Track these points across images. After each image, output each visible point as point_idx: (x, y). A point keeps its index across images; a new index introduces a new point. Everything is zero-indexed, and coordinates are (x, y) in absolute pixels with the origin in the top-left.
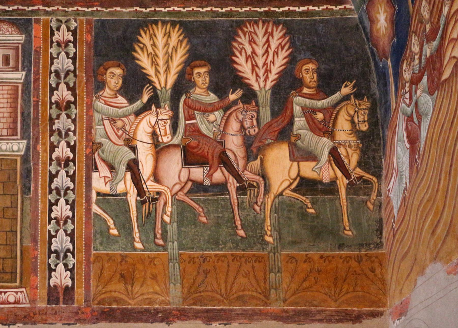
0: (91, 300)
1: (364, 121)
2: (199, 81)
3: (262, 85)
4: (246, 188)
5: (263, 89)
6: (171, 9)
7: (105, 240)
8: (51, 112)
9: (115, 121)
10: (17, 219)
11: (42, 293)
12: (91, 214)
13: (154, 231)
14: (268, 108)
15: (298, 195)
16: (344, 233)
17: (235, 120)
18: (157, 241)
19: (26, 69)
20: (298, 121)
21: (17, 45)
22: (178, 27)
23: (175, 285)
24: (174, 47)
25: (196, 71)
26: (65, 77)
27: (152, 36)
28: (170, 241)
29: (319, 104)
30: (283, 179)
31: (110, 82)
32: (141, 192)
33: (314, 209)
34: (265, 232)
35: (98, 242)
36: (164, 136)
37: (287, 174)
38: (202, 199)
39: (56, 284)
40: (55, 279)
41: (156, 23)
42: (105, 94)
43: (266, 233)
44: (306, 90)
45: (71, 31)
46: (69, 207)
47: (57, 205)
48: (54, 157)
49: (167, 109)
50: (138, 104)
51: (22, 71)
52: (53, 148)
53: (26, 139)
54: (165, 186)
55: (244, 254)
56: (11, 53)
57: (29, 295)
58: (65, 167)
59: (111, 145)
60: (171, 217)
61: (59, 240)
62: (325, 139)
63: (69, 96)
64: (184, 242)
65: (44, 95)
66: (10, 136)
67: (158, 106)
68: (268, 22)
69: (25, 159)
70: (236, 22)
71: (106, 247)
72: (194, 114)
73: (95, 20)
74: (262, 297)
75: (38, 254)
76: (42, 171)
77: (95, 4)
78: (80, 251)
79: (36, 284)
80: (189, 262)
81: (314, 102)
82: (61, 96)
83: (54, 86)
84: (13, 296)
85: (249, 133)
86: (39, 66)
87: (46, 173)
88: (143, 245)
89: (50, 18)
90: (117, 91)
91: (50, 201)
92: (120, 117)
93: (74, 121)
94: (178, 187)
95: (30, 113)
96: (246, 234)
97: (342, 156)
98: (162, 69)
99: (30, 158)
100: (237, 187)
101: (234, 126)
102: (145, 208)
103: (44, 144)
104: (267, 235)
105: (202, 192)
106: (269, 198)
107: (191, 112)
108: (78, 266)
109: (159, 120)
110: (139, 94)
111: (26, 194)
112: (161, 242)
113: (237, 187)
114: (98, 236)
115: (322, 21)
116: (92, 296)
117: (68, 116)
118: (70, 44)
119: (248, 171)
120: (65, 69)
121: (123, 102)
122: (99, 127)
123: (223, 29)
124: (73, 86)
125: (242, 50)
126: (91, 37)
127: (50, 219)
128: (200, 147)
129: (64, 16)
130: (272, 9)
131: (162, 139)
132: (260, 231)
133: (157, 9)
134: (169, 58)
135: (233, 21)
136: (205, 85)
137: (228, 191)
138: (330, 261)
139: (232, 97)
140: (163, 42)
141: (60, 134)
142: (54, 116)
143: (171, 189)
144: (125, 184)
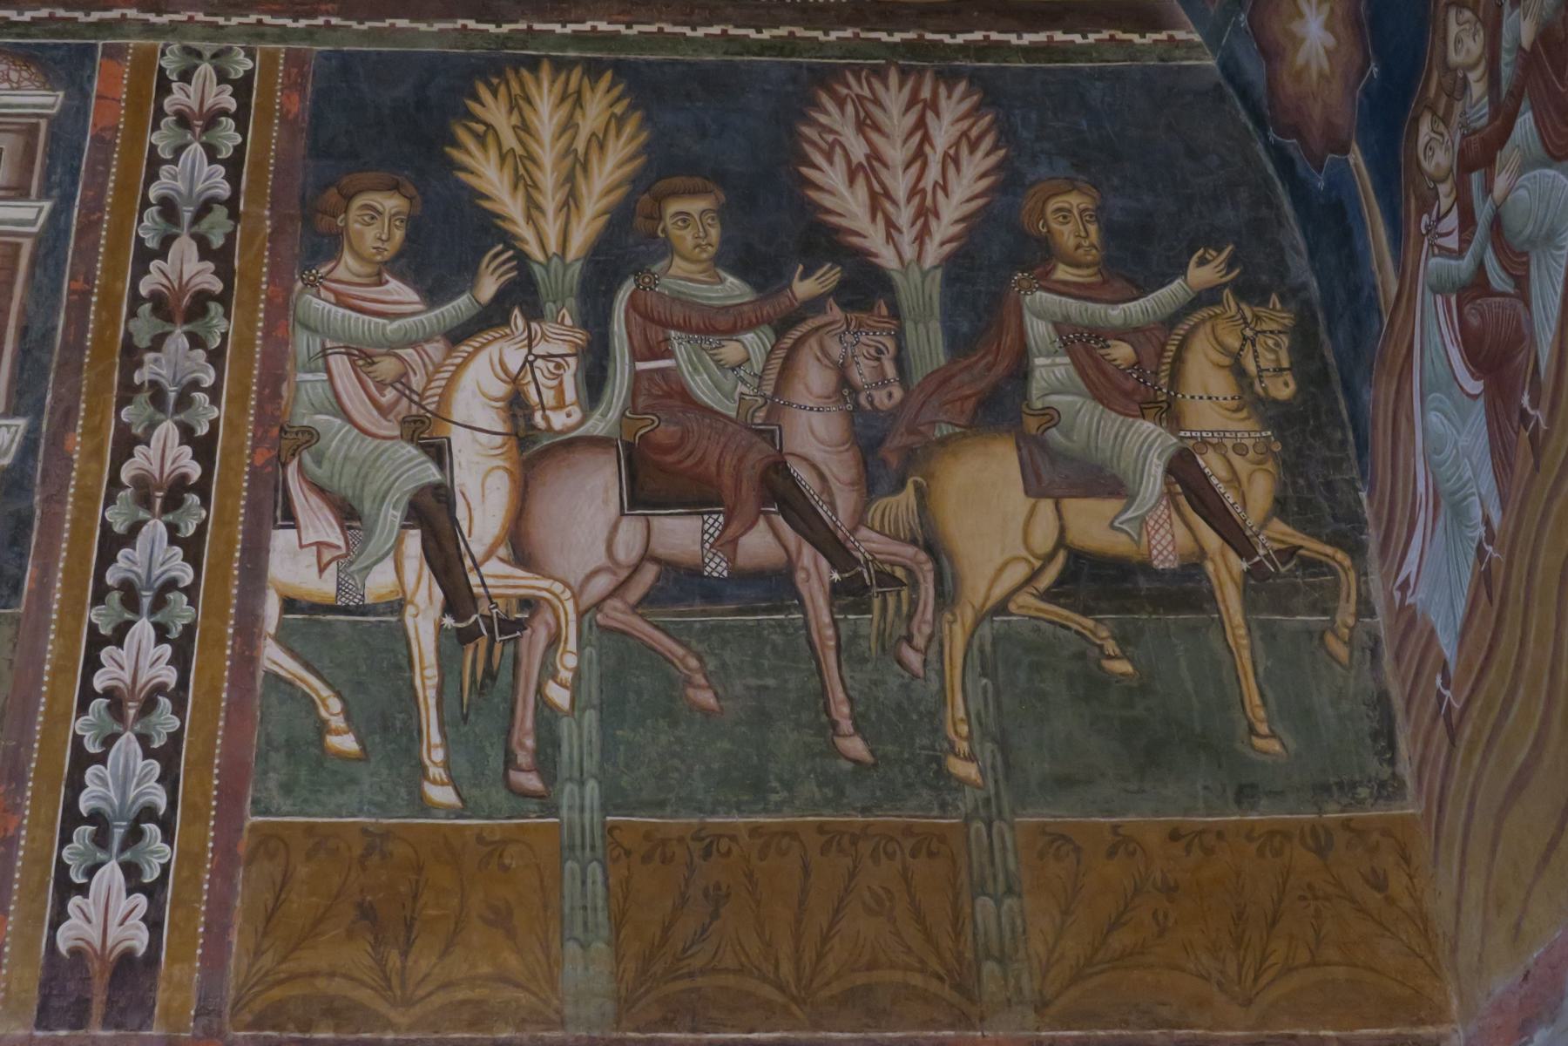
0: (227, 1010)
1: (1279, 370)
2: (686, 238)
3: (909, 252)
4: (866, 588)
5: (914, 268)
6: (587, 27)
7: (303, 774)
9: (369, 359)
12: (253, 676)
13: (508, 741)
14: (935, 325)
15: (1065, 612)
16: (1252, 746)
17: (819, 360)
18: (515, 776)
19: (55, 192)
20: (1043, 366)
21: (34, 120)
22: (608, 76)
23: (584, 946)
24: (593, 134)
25: (673, 207)
26: (198, 218)
27: (519, 103)
28: (570, 779)
29: (1116, 314)
30: (1007, 556)
31: (361, 234)
32: (457, 599)
33: (1131, 660)
34: (946, 745)
35: (274, 779)
36: (553, 409)
37: (1019, 541)
38: (697, 626)
39: (81, 944)
41: (533, 64)
42: (340, 273)
43: (952, 746)
44: (1063, 273)
46: (167, 650)
47: (120, 644)
48: (126, 474)
49: (568, 321)
50: (459, 307)
51: (39, 198)
52: (126, 444)
53: (24, 415)
54: (556, 580)
55: (869, 825)
58: (166, 509)
59: (350, 439)
60: (575, 687)
61: (114, 775)
62: (1147, 426)
63: (205, 277)
64: (625, 781)
65: (114, 272)
67: (534, 313)
68: (921, 72)
70: (811, 68)
71: (306, 801)
72: (667, 339)
73: (320, 52)
74: (946, 992)
75: (20, 827)
77: (323, 7)
78: (196, 814)
80: (646, 859)
81: (1098, 309)
83: (152, 243)
85: (872, 403)
86: (103, 186)
87: (91, 532)
88: (459, 794)
89: (161, 44)
90: (385, 263)
91: (93, 628)
92: (391, 347)
93: (216, 357)
94: (603, 583)
95: (55, 328)
96: (872, 752)
97: (1214, 481)
98: (550, 202)
99: (31, 478)
100: (833, 583)
101: (814, 378)
102: (472, 658)
103: (94, 431)
104: (957, 755)
105: (697, 601)
106: (955, 621)
107: (655, 333)
108: (185, 874)
109: (537, 357)
110: (467, 273)
112: (532, 782)
113: (833, 583)
114: (277, 758)
115: (1101, 74)
116: (232, 993)
117: (196, 341)
118: (223, 119)
119: (872, 529)
120: (200, 195)
121: (406, 299)
122: (309, 377)
123: (767, 87)
124: (223, 246)
125: (832, 146)
127: (88, 695)
128: (689, 448)
129: (211, 39)
130: (929, 36)
131: (546, 418)
132: (926, 742)
133: (537, 26)
134: (575, 169)
135: (800, 65)
136: (704, 251)
137: (798, 596)
138: (1208, 851)
139: (804, 289)
140: (555, 120)
142: (142, 340)
143: (576, 589)
144: (398, 569)
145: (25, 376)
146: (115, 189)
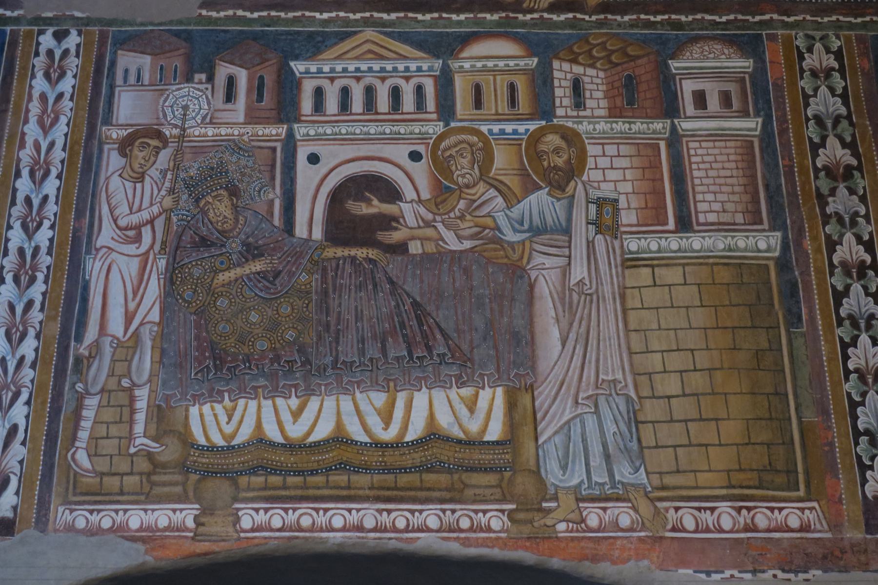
8: (818, 185)
10: (783, 371)
11: (852, 510)
19: (762, 113)
21: (742, 75)
26: (835, 126)
40: (874, 483)
45: (833, 53)
47: (856, 347)
48: (836, 261)
51: (755, 117)
52: (832, 245)
53: (779, 230)
56: (732, 88)
57: (827, 515)
61: (871, 411)
63: (846, 157)
66: (749, 224)
69: (783, 264)
75: (833, 437)
76: (818, 285)
77: (868, 11)
79: (838, 496)
82: (832, 158)
83: (816, 140)
84: (796, 517)
86: (785, 109)
87: (827, 290)
89: (794, 33)
91: (841, 339)
93: (863, 199)
95: (781, 185)
103: (815, 238)
111: (795, 326)
117: (852, 191)
120: (832, 114)
126: (869, 61)
127: (847, 373)
129: (817, 30)
141: (840, 220)
142: (825, 191)
145: (774, 210)
146: (791, 111)
